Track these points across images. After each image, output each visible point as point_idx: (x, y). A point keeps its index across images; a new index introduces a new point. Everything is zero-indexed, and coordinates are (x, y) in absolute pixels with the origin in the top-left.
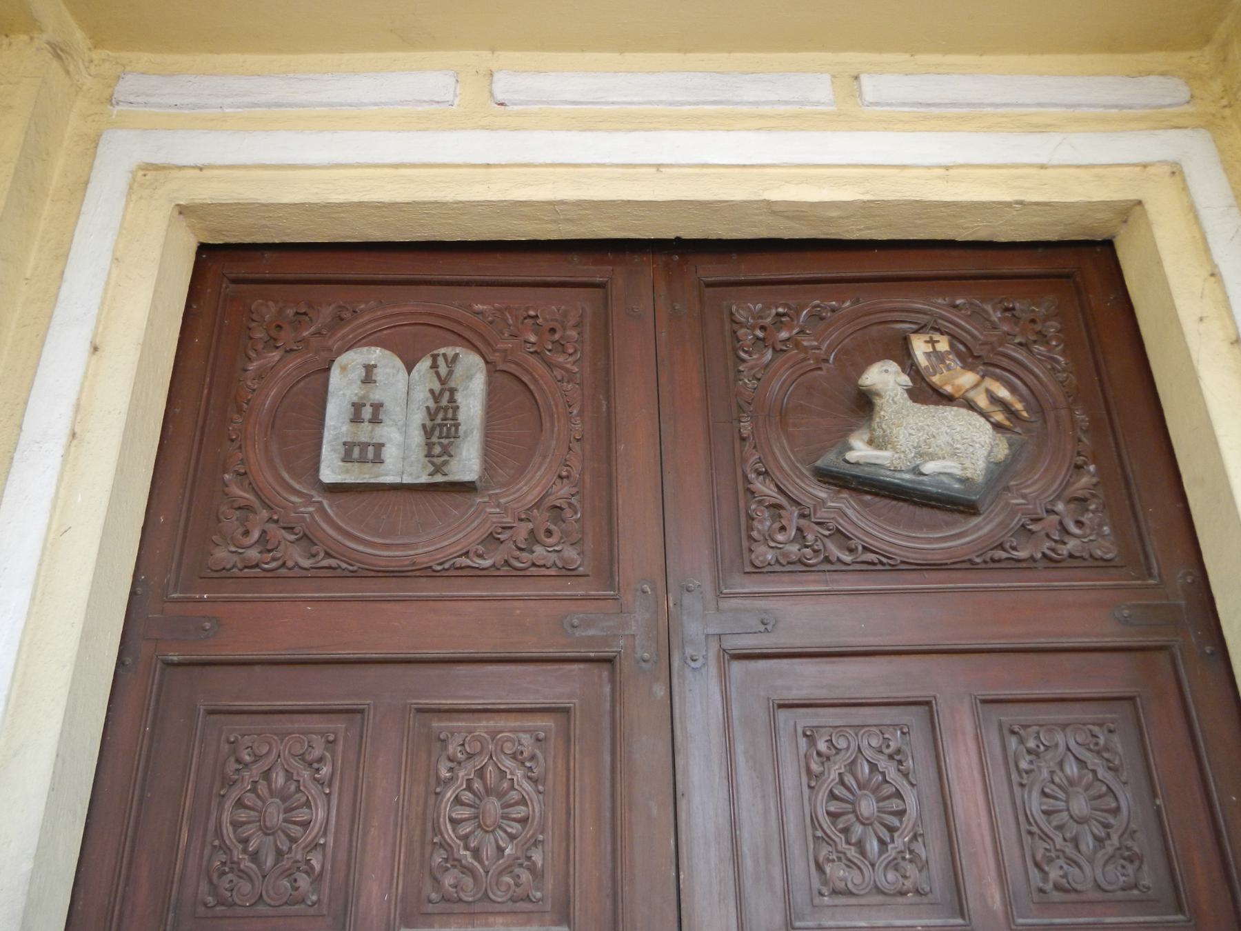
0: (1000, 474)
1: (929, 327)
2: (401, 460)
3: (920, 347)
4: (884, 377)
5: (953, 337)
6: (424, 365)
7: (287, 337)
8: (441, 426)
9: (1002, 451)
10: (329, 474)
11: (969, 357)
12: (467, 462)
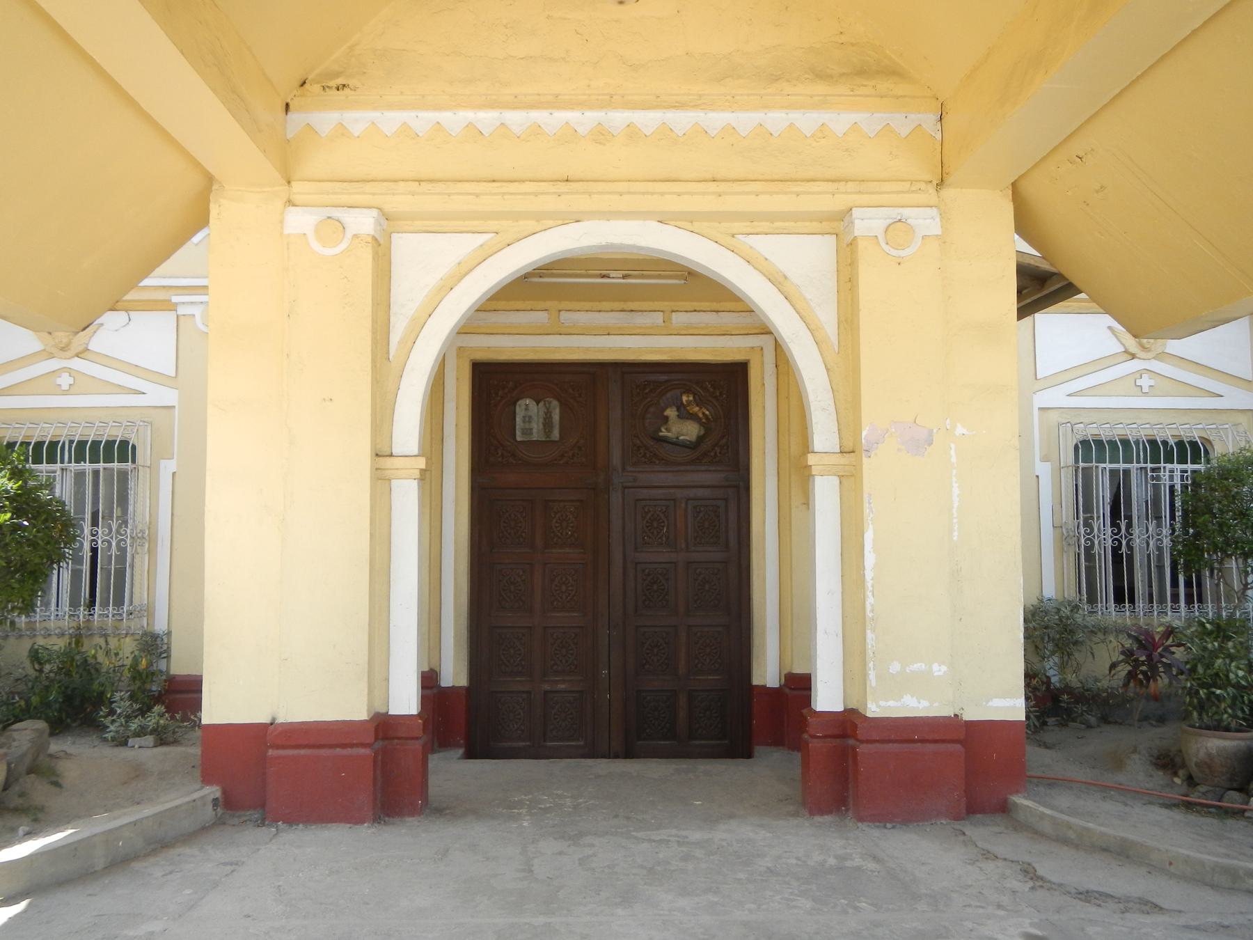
0: (700, 439)
1: (688, 391)
2: (537, 434)
3: (685, 398)
4: (671, 413)
5: (694, 395)
6: (541, 404)
7: (500, 393)
8: (548, 424)
9: (702, 432)
10: (519, 439)
11: (699, 402)
12: (556, 434)
